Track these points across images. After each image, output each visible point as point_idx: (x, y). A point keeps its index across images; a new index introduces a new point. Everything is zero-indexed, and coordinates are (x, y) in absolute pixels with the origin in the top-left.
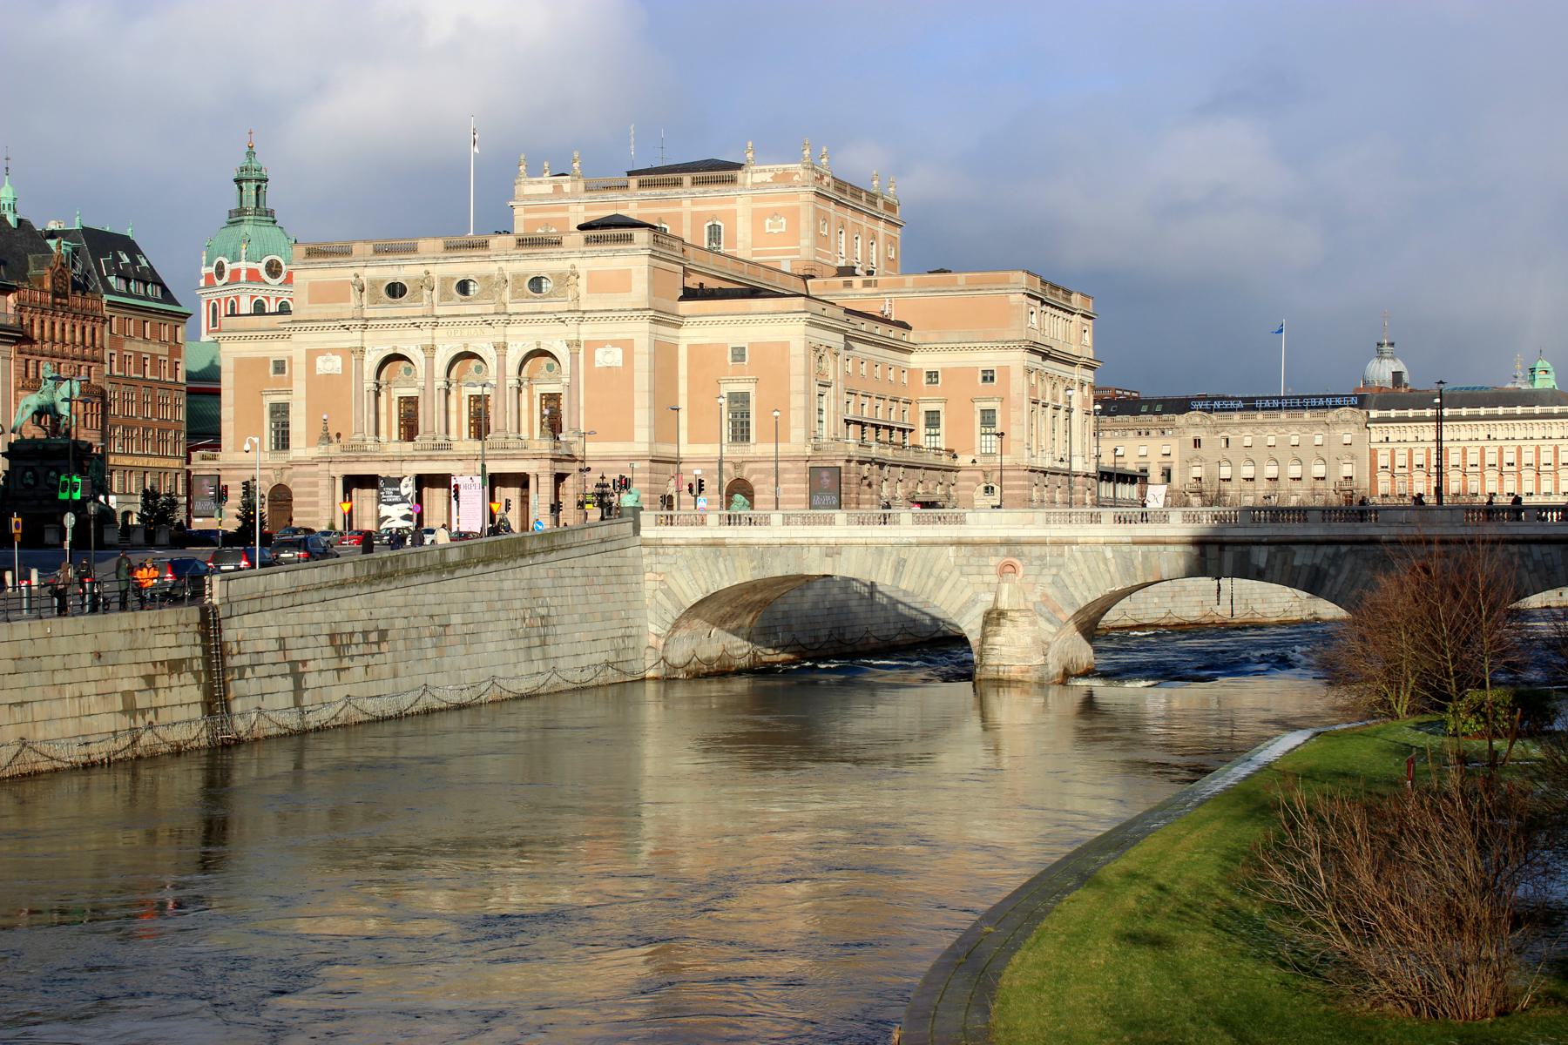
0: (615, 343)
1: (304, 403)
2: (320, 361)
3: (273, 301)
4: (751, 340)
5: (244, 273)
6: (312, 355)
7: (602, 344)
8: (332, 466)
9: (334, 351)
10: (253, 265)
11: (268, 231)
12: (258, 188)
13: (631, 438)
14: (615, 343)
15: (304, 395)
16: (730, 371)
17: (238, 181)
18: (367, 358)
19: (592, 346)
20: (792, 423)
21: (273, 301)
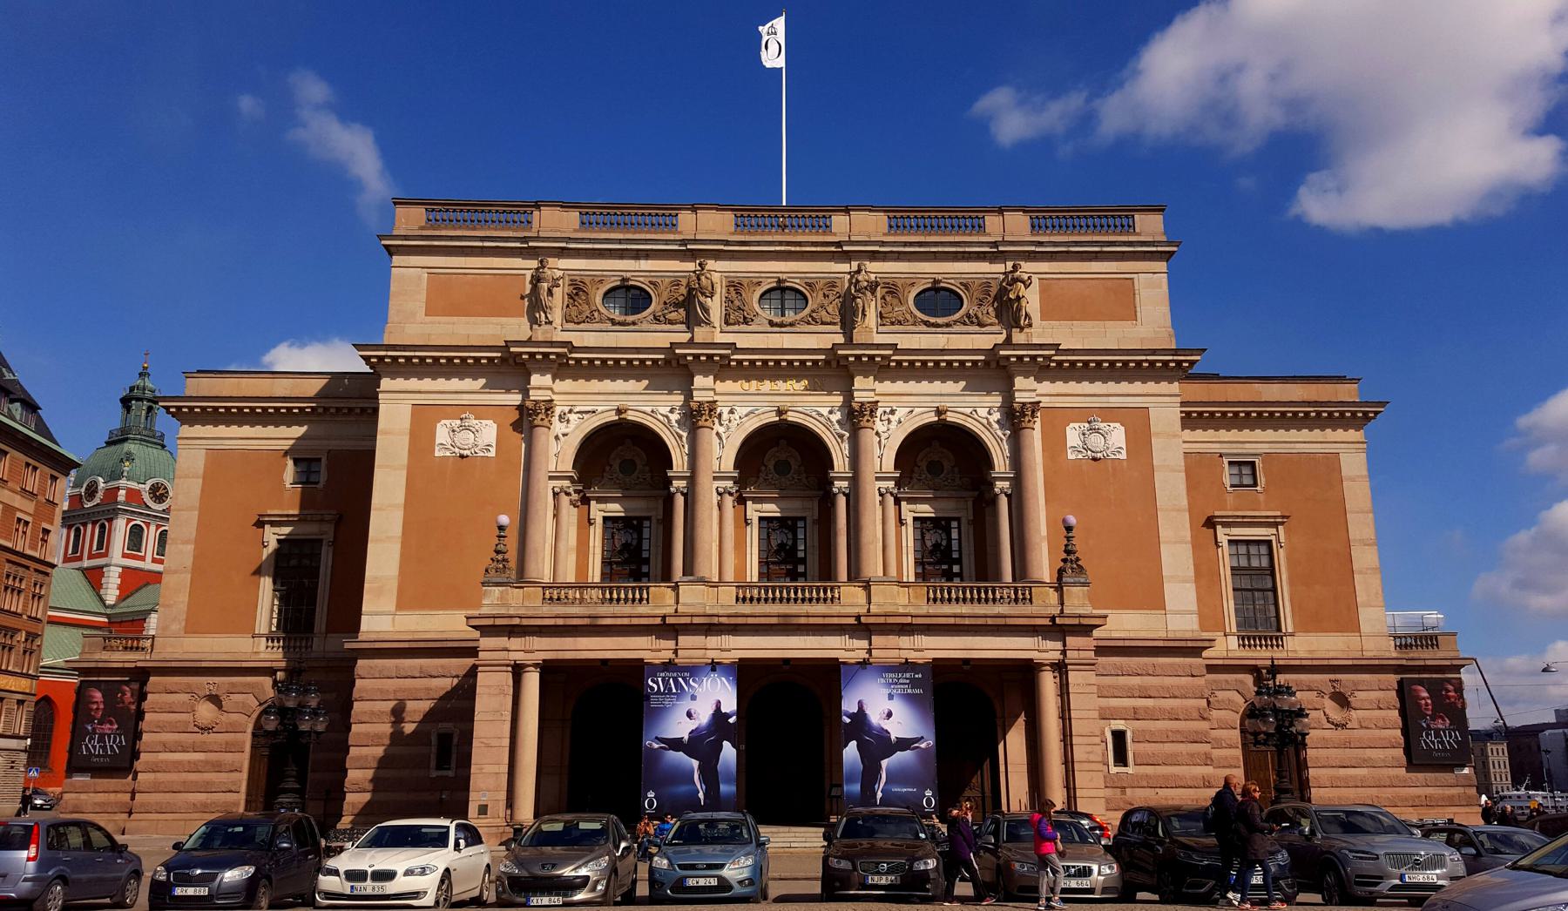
0: (1110, 414)
1: (399, 515)
2: (442, 433)
3: (153, 528)
4: (1265, 448)
5: (122, 492)
6: (424, 418)
7: (1082, 414)
8: (515, 643)
9: (481, 411)
10: (133, 485)
11: (155, 452)
12: (150, 409)
13: (1154, 599)
14: (1110, 414)
15: (400, 496)
16: (1230, 499)
17: (126, 402)
18: (558, 427)
19: (1058, 419)
20: (1361, 597)
21: (153, 528)
